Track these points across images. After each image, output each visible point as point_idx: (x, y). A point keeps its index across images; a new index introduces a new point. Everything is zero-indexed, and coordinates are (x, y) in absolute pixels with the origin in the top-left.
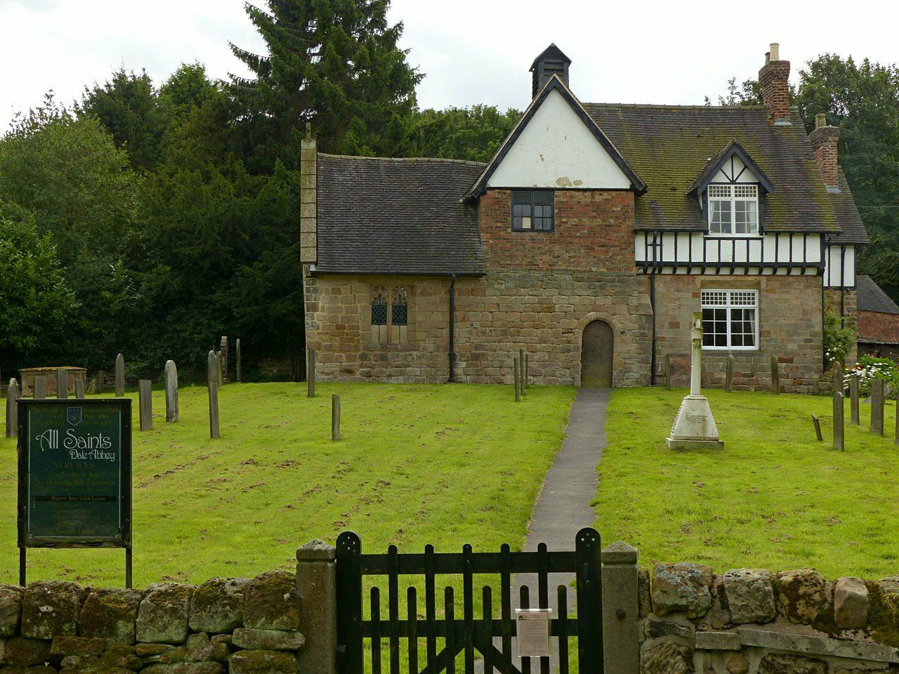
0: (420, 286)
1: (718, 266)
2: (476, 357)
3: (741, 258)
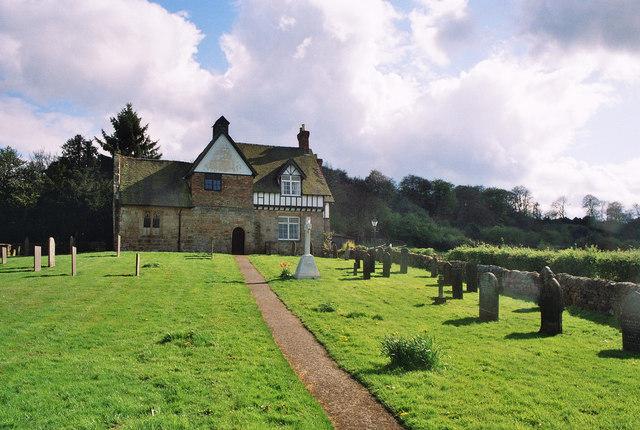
0: (166, 211)
1: (285, 207)
2: (189, 241)
3: (294, 204)
